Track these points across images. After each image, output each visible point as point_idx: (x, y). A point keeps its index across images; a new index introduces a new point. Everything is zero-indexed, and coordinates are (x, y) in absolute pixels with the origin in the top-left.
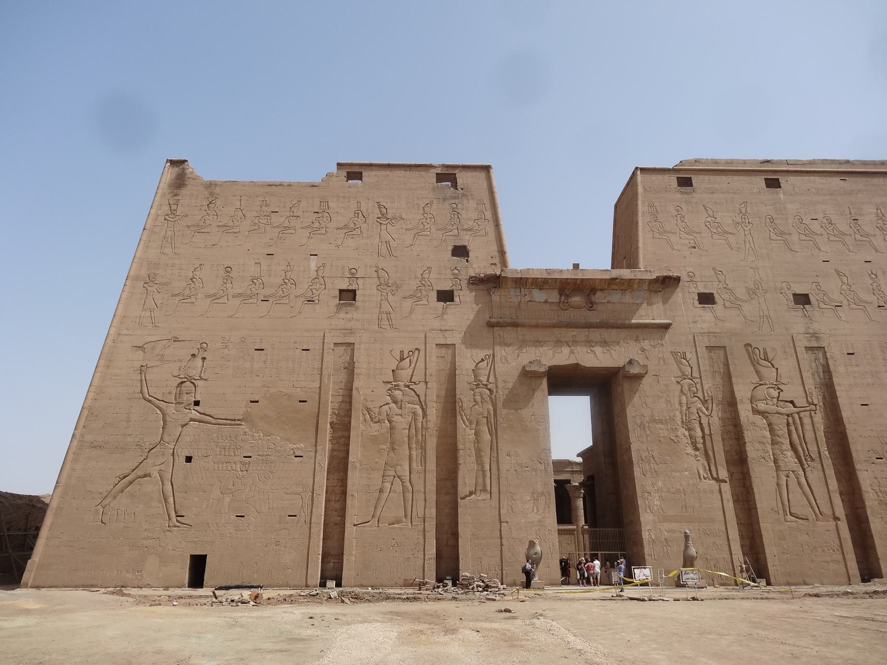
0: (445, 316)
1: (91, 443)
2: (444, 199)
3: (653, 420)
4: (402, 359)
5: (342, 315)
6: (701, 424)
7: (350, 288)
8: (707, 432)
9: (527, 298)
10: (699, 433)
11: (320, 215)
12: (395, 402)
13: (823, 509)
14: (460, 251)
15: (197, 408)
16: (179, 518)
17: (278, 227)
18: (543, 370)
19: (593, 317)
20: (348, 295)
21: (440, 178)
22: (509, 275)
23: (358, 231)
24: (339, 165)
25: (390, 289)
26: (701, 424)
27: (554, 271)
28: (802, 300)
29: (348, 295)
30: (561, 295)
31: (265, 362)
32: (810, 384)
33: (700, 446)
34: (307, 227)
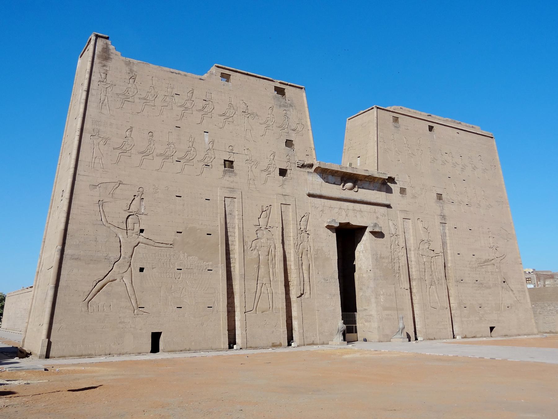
0: (285, 186)
1: (72, 256)
2: (280, 106)
5: (227, 178)
7: (230, 159)
11: (207, 103)
14: (289, 143)
16: (140, 309)
17: (181, 106)
18: (337, 225)
23: (230, 119)
25: (253, 163)
29: (229, 164)
30: (342, 180)
31: (183, 205)
34: (200, 110)
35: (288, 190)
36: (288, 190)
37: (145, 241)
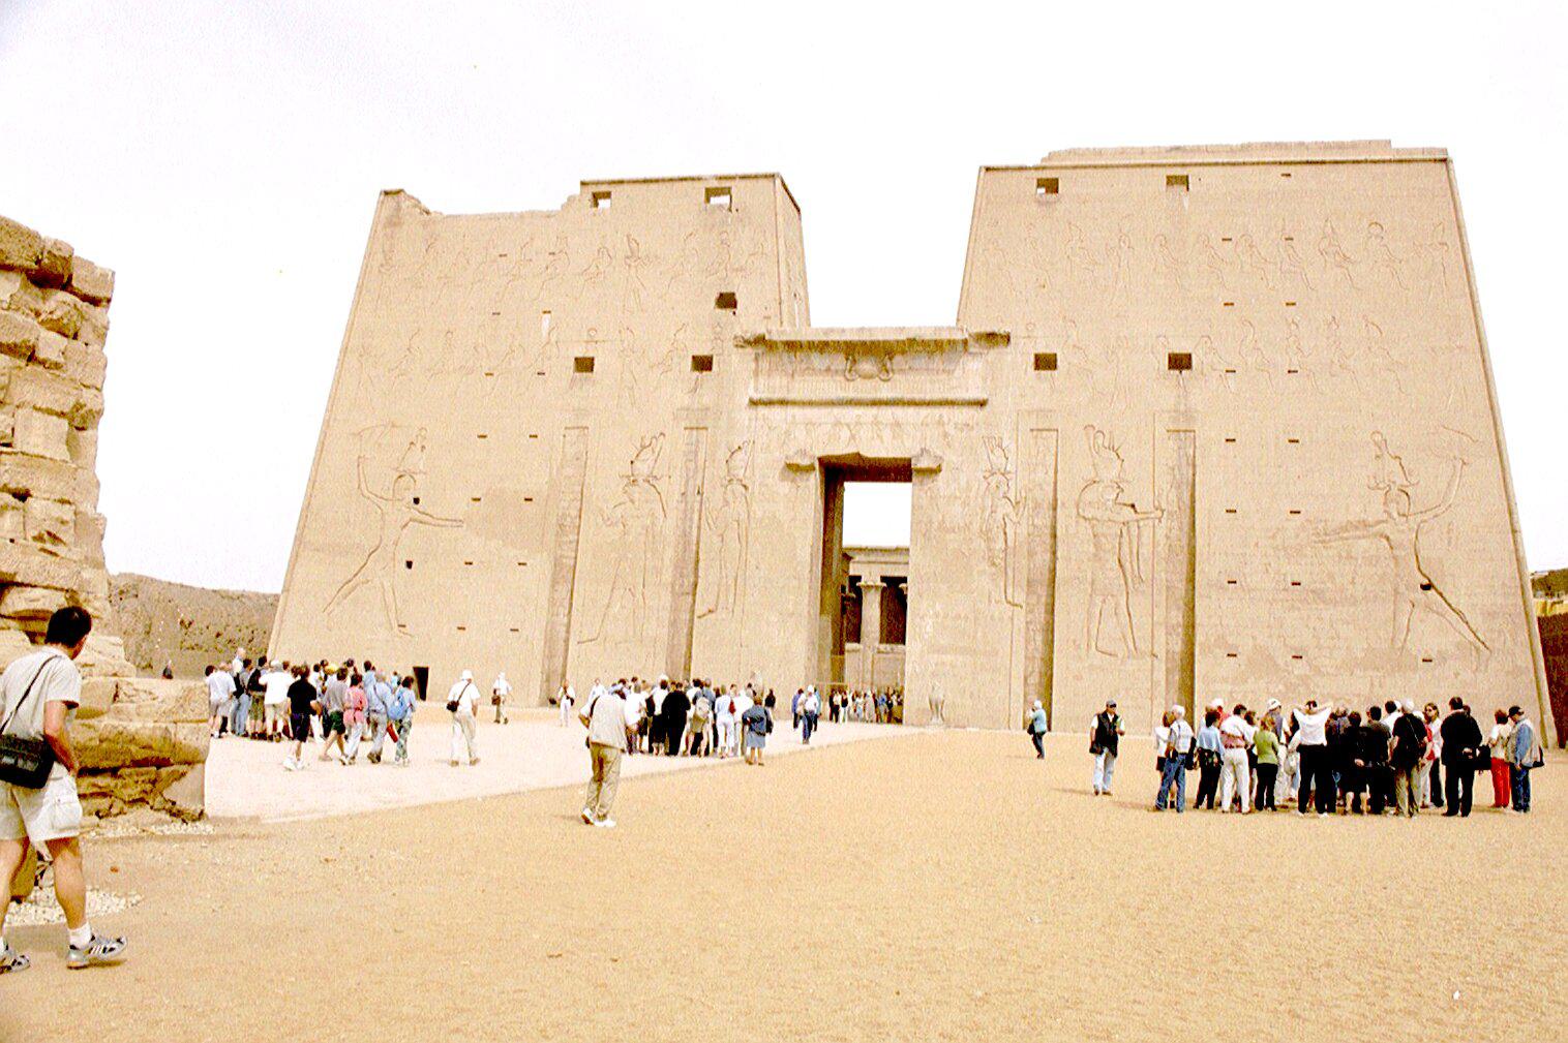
3: (942, 527)
4: (643, 447)
6: (1005, 533)
8: (1010, 543)
9: (804, 366)
10: (1000, 545)
12: (632, 501)
13: (1141, 645)
14: (727, 301)
15: (415, 506)
19: (885, 392)
20: (585, 365)
21: (711, 193)
22: (775, 337)
24: (583, 184)
26: (1005, 533)
27: (832, 330)
28: (1180, 362)
29: (585, 365)
30: (847, 359)
32: (1164, 482)
33: (997, 561)
35: (706, 398)
36: (706, 398)
37: (418, 516)
